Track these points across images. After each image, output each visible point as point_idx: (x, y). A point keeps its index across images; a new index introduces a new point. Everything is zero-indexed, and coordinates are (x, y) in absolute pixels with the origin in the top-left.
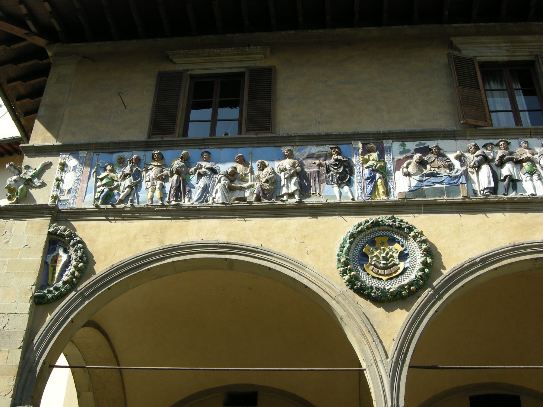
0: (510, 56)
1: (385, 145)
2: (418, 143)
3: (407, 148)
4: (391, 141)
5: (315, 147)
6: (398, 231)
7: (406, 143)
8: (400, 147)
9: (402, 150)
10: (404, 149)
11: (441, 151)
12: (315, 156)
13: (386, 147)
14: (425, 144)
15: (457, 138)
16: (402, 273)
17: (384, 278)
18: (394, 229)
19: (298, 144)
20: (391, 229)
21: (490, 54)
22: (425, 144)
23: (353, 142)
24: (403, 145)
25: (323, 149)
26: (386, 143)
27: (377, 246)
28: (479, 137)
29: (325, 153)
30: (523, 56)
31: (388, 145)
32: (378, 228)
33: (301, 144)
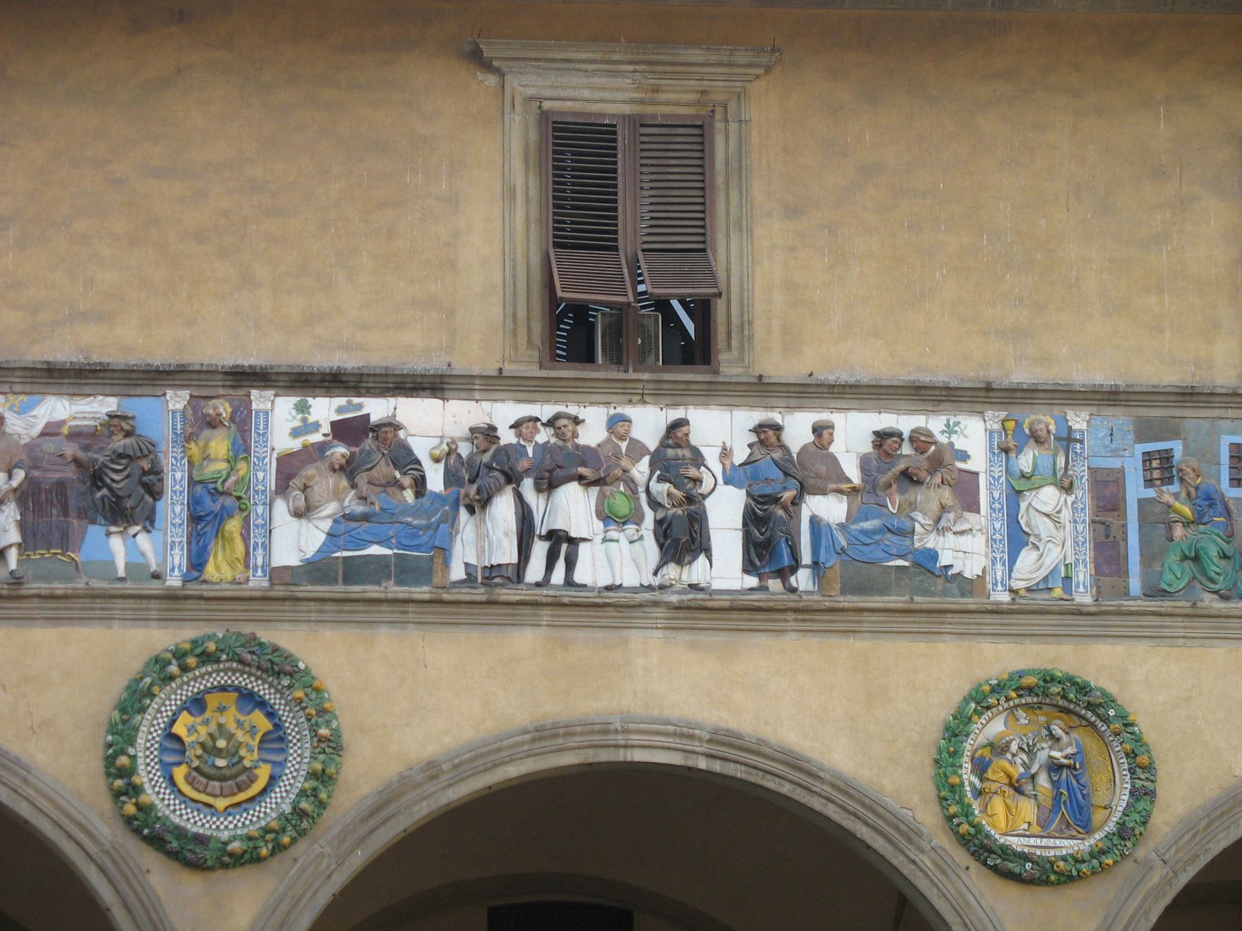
0: (641, 102)
1: (254, 406)
2: (342, 401)
3: (311, 419)
4: (270, 393)
5: (65, 402)
6: (265, 676)
7: (310, 400)
8: (294, 412)
9: (297, 423)
10: (304, 420)
11: (402, 434)
12: (65, 430)
13: (257, 412)
14: (360, 406)
15: (447, 394)
16: (264, 791)
17: (221, 803)
18: (253, 670)
19: (18, 388)
20: (247, 669)
21: (586, 94)
22: (360, 406)
23: (170, 393)
24: (303, 408)
25: (87, 409)
26: (260, 399)
27: (208, 714)
28: (505, 395)
29: (92, 423)
30: (677, 104)
31: (262, 406)
32: (215, 666)
33: (28, 388)
